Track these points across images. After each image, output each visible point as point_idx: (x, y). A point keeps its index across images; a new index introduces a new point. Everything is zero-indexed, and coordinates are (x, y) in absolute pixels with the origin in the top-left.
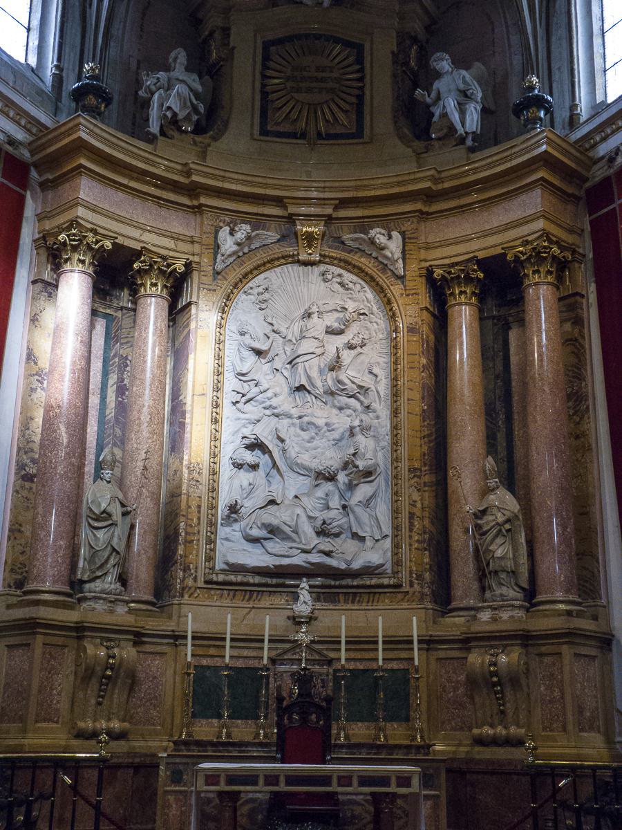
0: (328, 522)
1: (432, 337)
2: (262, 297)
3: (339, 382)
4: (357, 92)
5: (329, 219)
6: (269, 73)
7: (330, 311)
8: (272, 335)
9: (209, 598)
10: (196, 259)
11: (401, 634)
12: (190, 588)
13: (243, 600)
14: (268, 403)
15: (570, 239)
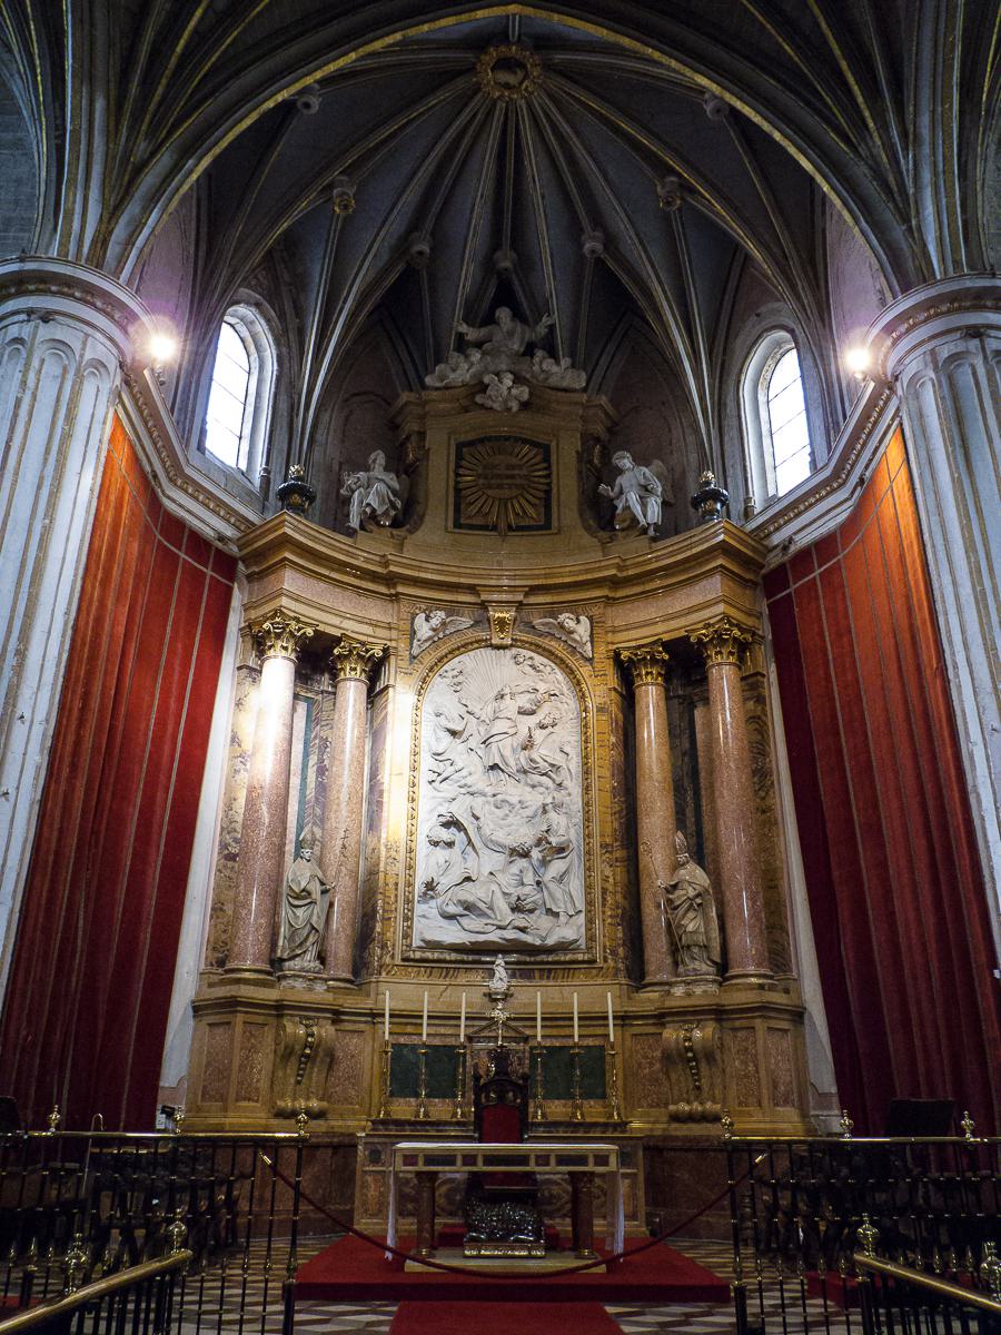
0: (522, 898)
1: (620, 716)
2: (456, 680)
4: (545, 488)
6: (461, 471)
8: (467, 716)
10: (393, 644)
11: (597, 1010)
14: (463, 782)
15: (750, 622)
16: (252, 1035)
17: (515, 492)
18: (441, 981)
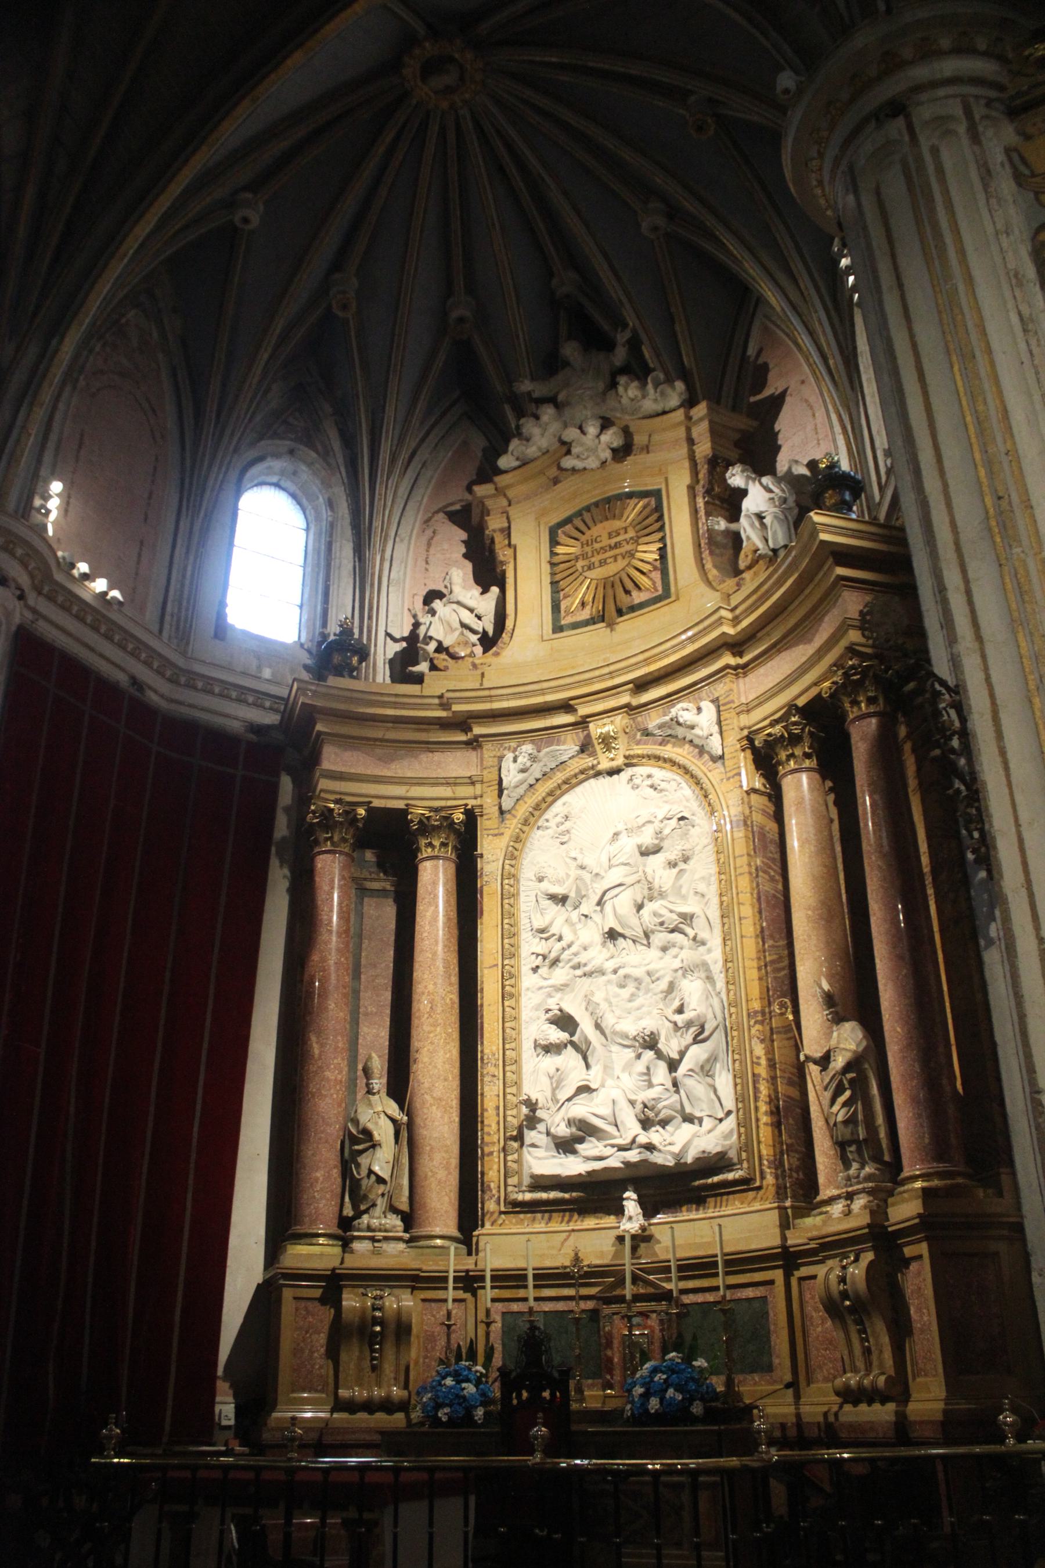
2: (562, 828)
3: (655, 915)
5: (629, 709)
7: (644, 825)
9: (517, 1223)
10: (478, 802)
12: (493, 1213)
13: (562, 1222)
14: (576, 960)
16: (308, 1312)
17: (621, 563)
18: (564, 1227)
